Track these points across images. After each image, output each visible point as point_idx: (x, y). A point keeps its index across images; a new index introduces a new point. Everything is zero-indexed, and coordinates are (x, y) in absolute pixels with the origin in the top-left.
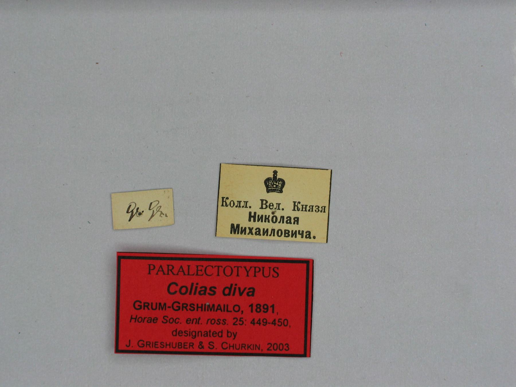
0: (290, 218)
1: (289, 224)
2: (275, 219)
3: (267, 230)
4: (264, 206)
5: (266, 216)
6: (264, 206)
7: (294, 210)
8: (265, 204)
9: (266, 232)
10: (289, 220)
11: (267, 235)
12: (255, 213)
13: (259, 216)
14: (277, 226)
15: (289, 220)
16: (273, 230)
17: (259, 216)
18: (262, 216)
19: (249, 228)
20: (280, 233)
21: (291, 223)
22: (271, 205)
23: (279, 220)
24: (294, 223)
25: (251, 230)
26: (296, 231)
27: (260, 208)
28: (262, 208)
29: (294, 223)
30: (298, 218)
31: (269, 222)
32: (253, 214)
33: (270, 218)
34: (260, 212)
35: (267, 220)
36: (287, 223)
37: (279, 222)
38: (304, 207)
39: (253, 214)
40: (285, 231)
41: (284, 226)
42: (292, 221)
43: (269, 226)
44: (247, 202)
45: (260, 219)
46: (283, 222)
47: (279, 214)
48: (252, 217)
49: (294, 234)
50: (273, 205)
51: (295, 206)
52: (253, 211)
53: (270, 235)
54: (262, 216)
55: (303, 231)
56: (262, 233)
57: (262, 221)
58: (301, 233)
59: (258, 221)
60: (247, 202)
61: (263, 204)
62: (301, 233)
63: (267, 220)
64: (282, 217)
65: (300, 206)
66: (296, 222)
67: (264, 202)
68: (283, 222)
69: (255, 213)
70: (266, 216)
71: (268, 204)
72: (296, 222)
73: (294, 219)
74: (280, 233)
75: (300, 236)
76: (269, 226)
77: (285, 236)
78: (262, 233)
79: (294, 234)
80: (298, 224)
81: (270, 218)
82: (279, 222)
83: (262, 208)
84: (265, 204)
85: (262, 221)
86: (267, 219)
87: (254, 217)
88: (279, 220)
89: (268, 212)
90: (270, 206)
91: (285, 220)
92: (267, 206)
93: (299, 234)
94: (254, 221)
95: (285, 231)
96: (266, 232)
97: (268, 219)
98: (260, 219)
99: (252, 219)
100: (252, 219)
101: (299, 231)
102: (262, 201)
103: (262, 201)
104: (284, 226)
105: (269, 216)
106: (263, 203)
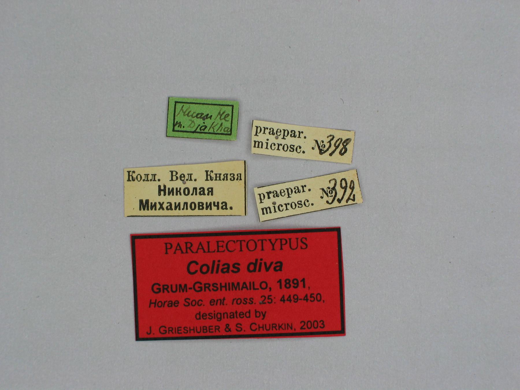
0: (204, 189)
1: (202, 195)
2: (187, 192)
3: (179, 203)
4: (174, 178)
5: (177, 189)
6: (174, 178)
7: (207, 180)
8: (175, 176)
9: (178, 206)
10: (202, 191)
11: (179, 209)
12: (165, 186)
13: (169, 189)
14: (190, 199)
15: (202, 191)
16: (186, 203)
17: (169, 189)
18: (173, 189)
19: (159, 203)
20: (193, 206)
21: (204, 194)
22: (182, 176)
23: (191, 192)
24: (208, 194)
25: (161, 205)
26: (211, 203)
27: (170, 181)
28: (172, 180)
29: (208, 194)
30: (212, 189)
31: (180, 194)
32: (162, 188)
33: (182, 191)
34: (170, 185)
35: (178, 193)
36: (200, 194)
37: (192, 194)
38: (218, 176)
39: (162, 188)
40: (199, 203)
41: (197, 199)
42: (206, 192)
43: (181, 199)
44: (155, 175)
45: (171, 192)
46: (196, 194)
47: (191, 185)
48: (162, 190)
49: (209, 206)
50: (184, 177)
51: (207, 175)
52: (161, 184)
53: (183, 209)
54: (173, 189)
55: (218, 203)
56: (173, 207)
57: (173, 195)
58: (216, 204)
59: (169, 194)
60: (155, 175)
61: (173, 176)
62: (216, 204)
63: (178, 193)
64: (195, 189)
65: (213, 175)
66: (210, 193)
67: (174, 173)
68: (196, 194)
69: (165, 186)
70: (177, 189)
71: (178, 176)
72: (210, 193)
73: (208, 189)
74: (193, 206)
75: (216, 208)
76: (181, 199)
77: (199, 209)
78: (173, 207)
79: (209, 206)
80: (212, 195)
81: (182, 191)
82: (192, 194)
83: (172, 180)
84: (175, 176)
85: (173, 195)
86: (178, 191)
87: (164, 190)
88: (191, 192)
89: (178, 184)
90: (181, 177)
91: (198, 191)
92: (177, 178)
93: (215, 205)
94: (165, 195)
95: (199, 203)
96: (178, 206)
97: (180, 191)
98: (171, 192)
99: (162, 193)
100: (162, 193)
101: (214, 203)
102: (172, 172)
103: (172, 172)
104: (197, 199)
105: (180, 189)
106: (173, 175)
